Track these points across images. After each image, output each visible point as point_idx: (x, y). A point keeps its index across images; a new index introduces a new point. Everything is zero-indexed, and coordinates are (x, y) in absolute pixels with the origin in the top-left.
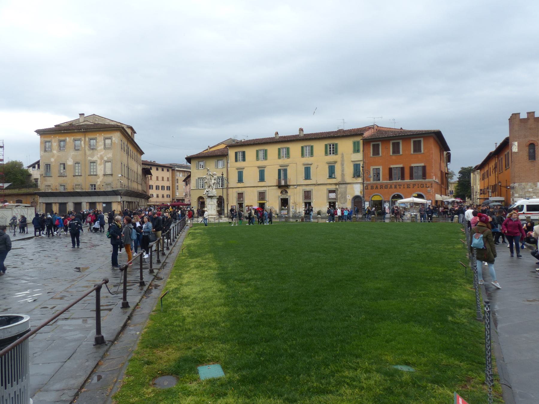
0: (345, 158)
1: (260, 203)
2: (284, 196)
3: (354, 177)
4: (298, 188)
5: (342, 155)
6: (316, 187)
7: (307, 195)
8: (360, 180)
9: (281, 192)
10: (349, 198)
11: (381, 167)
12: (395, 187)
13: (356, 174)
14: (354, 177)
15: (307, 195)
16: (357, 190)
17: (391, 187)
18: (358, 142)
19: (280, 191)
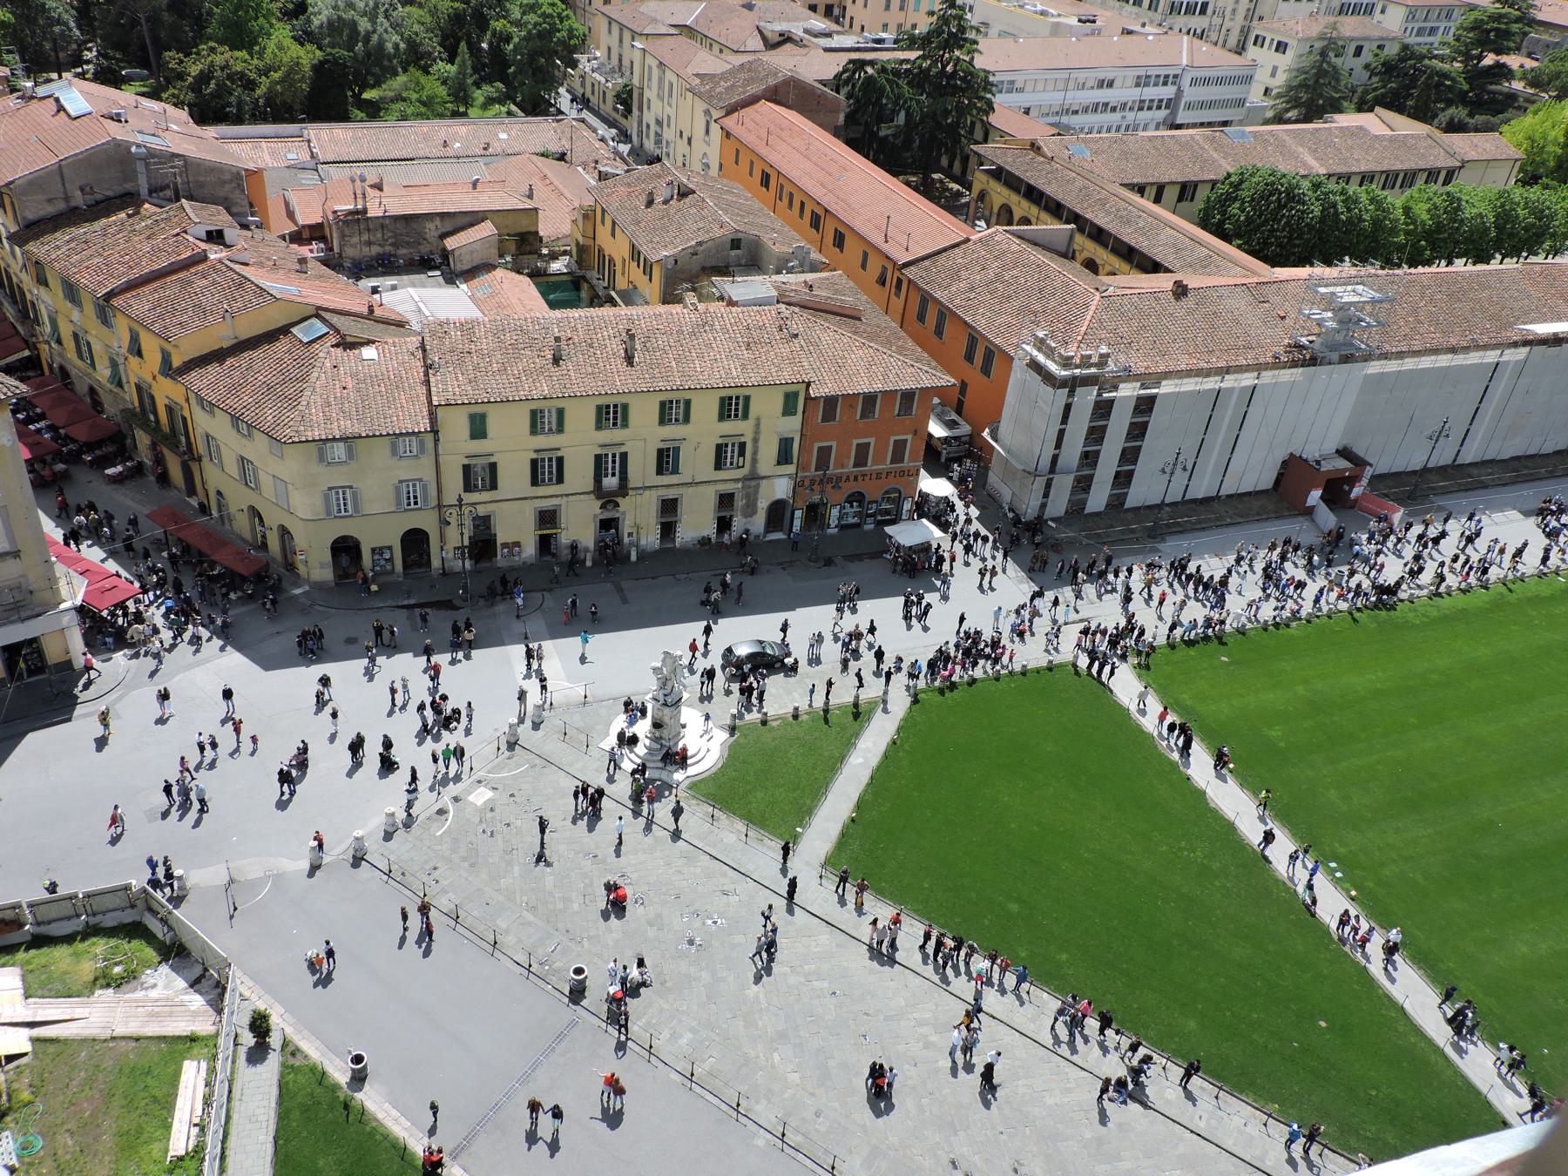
0: (763, 427)
1: (541, 536)
2: (607, 515)
3: (779, 463)
4: (647, 493)
5: (758, 419)
6: (691, 490)
7: (669, 507)
8: (791, 469)
9: (603, 507)
10: (763, 505)
11: (834, 444)
12: (856, 479)
13: (784, 457)
14: (779, 463)
15: (669, 507)
16: (780, 488)
17: (848, 479)
18: (796, 394)
19: (599, 503)
